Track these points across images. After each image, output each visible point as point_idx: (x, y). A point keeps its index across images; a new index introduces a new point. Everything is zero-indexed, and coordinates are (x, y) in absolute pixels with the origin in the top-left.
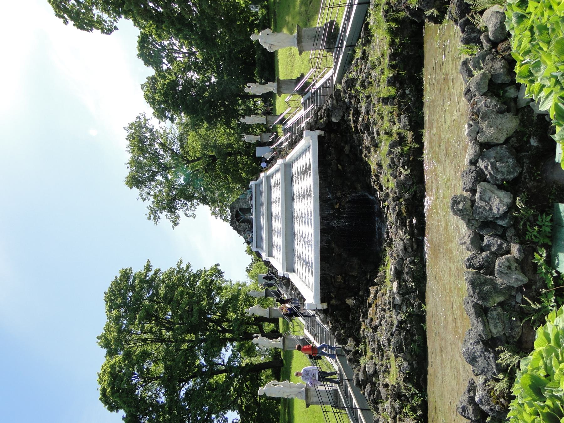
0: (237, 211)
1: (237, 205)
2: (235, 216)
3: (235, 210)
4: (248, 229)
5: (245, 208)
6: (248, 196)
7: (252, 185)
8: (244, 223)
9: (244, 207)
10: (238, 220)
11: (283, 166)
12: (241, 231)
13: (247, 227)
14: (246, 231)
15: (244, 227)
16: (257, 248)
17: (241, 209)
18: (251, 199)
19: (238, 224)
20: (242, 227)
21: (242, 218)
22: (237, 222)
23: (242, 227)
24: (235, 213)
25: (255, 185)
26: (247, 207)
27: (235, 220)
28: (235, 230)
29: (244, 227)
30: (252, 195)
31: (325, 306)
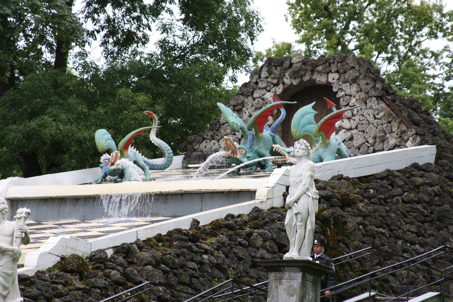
2: (306, 78)
3: (333, 77)
22: (279, 90)
24: (321, 79)
27: (287, 81)
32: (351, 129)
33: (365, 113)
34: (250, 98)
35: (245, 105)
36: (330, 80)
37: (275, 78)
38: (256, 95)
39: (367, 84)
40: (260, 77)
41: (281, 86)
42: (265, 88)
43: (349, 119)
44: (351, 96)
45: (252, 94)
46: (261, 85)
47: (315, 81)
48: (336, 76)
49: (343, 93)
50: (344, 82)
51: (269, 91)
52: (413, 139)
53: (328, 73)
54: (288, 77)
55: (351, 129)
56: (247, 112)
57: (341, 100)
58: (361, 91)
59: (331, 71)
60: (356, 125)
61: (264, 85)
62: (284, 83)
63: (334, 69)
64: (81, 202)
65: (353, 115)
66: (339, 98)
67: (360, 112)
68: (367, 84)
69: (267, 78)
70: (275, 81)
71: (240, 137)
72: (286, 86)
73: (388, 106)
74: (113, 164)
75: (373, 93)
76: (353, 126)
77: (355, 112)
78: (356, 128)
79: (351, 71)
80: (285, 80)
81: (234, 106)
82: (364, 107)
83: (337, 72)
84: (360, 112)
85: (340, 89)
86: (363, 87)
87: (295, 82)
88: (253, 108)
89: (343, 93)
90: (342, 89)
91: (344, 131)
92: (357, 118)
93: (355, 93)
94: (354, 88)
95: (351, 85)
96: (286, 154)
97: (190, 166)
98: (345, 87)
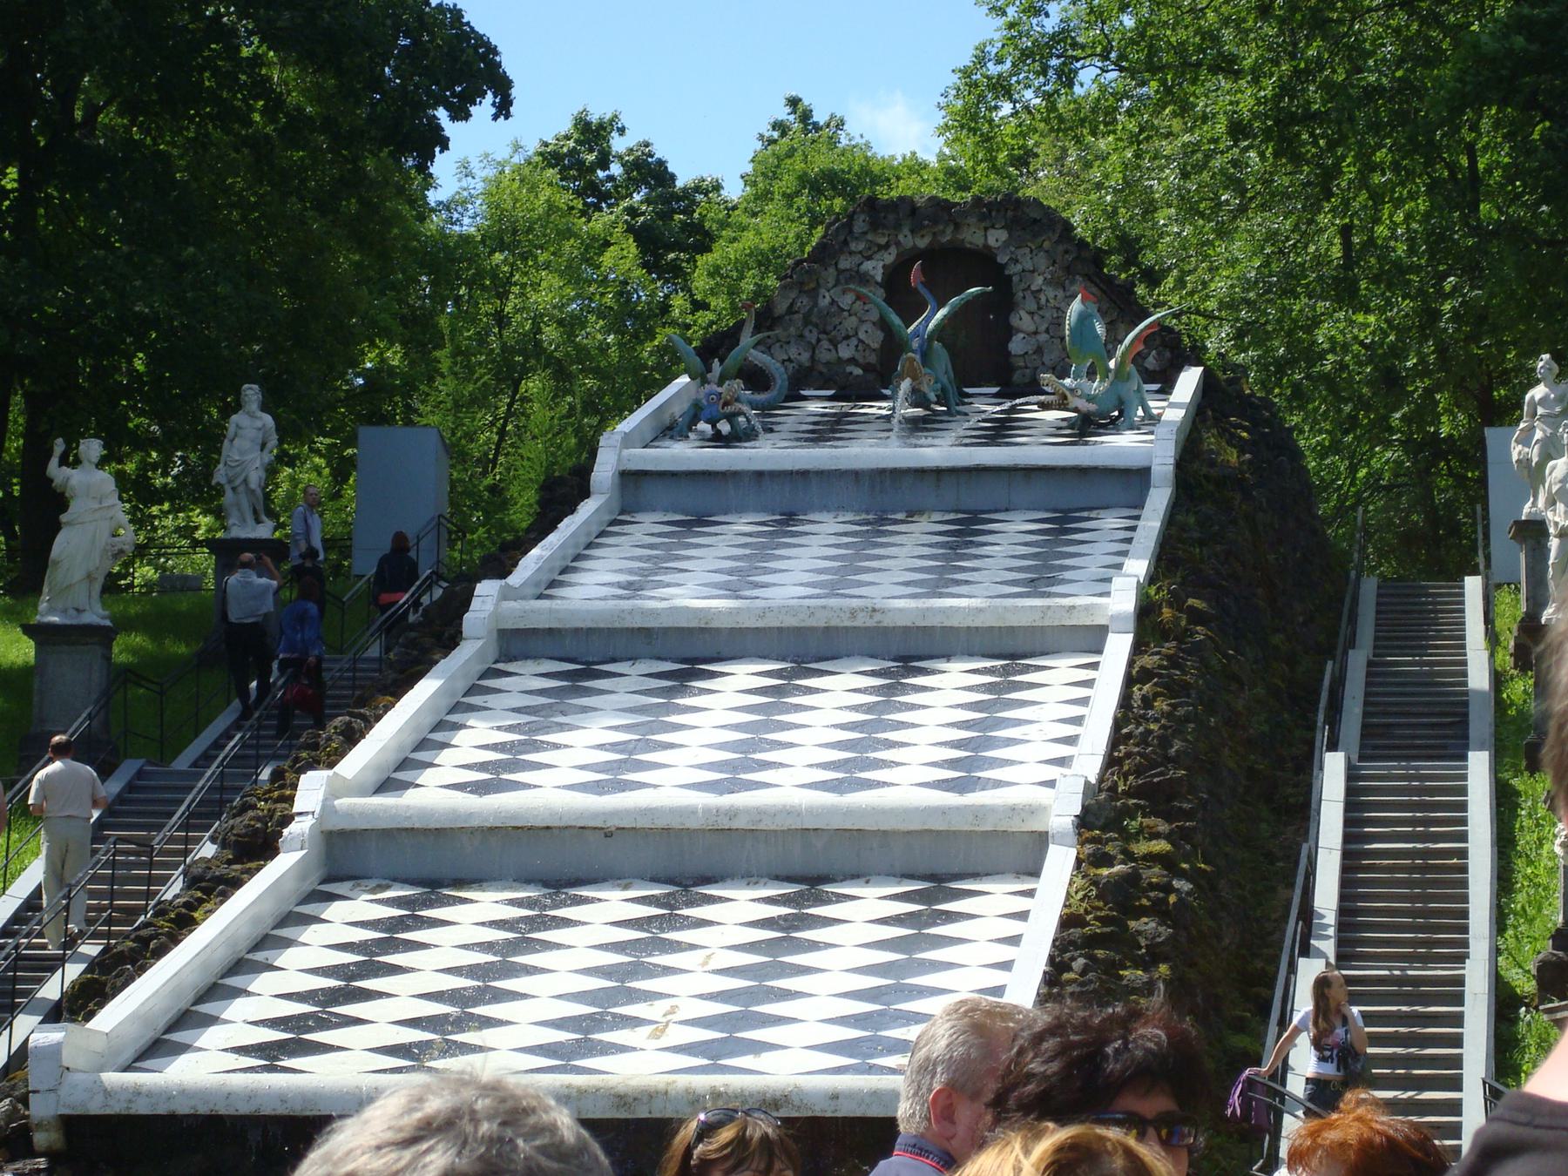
1: (1042, 261)
3: (996, 237)
4: (824, 355)
5: (1010, 332)
12: (813, 294)
13: (845, 352)
14: (812, 337)
17: (1003, 300)
19: (875, 268)
20: (846, 301)
22: (890, 257)
23: (846, 301)
24: (973, 236)
26: (1016, 346)
27: (907, 239)
32: (1036, 333)
34: (832, 270)
35: (821, 281)
36: (992, 242)
37: (883, 234)
39: (1066, 252)
40: (851, 232)
41: (893, 250)
42: (860, 252)
43: (1031, 314)
44: (1033, 272)
45: (836, 264)
46: (853, 246)
49: (1019, 267)
51: (869, 258)
52: (1158, 354)
53: (986, 229)
54: (908, 234)
55: (1036, 333)
56: (827, 294)
57: (1015, 279)
58: (1054, 262)
59: (993, 227)
60: (1046, 325)
61: (861, 246)
62: (898, 244)
65: (1040, 308)
66: (1010, 277)
68: (1066, 252)
69: (865, 233)
70: (883, 241)
71: (814, 341)
72: (901, 249)
73: (1104, 292)
74: (726, 404)
76: (1043, 328)
77: (1043, 301)
78: (1047, 331)
80: (901, 237)
85: (1011, 259)
88: (840, 288)
89: (1019, 267)
90: (1017, 261)
91: (1022, 335)
93: (1043, 268)
95: (1031, 251)
96: (1068, 393)
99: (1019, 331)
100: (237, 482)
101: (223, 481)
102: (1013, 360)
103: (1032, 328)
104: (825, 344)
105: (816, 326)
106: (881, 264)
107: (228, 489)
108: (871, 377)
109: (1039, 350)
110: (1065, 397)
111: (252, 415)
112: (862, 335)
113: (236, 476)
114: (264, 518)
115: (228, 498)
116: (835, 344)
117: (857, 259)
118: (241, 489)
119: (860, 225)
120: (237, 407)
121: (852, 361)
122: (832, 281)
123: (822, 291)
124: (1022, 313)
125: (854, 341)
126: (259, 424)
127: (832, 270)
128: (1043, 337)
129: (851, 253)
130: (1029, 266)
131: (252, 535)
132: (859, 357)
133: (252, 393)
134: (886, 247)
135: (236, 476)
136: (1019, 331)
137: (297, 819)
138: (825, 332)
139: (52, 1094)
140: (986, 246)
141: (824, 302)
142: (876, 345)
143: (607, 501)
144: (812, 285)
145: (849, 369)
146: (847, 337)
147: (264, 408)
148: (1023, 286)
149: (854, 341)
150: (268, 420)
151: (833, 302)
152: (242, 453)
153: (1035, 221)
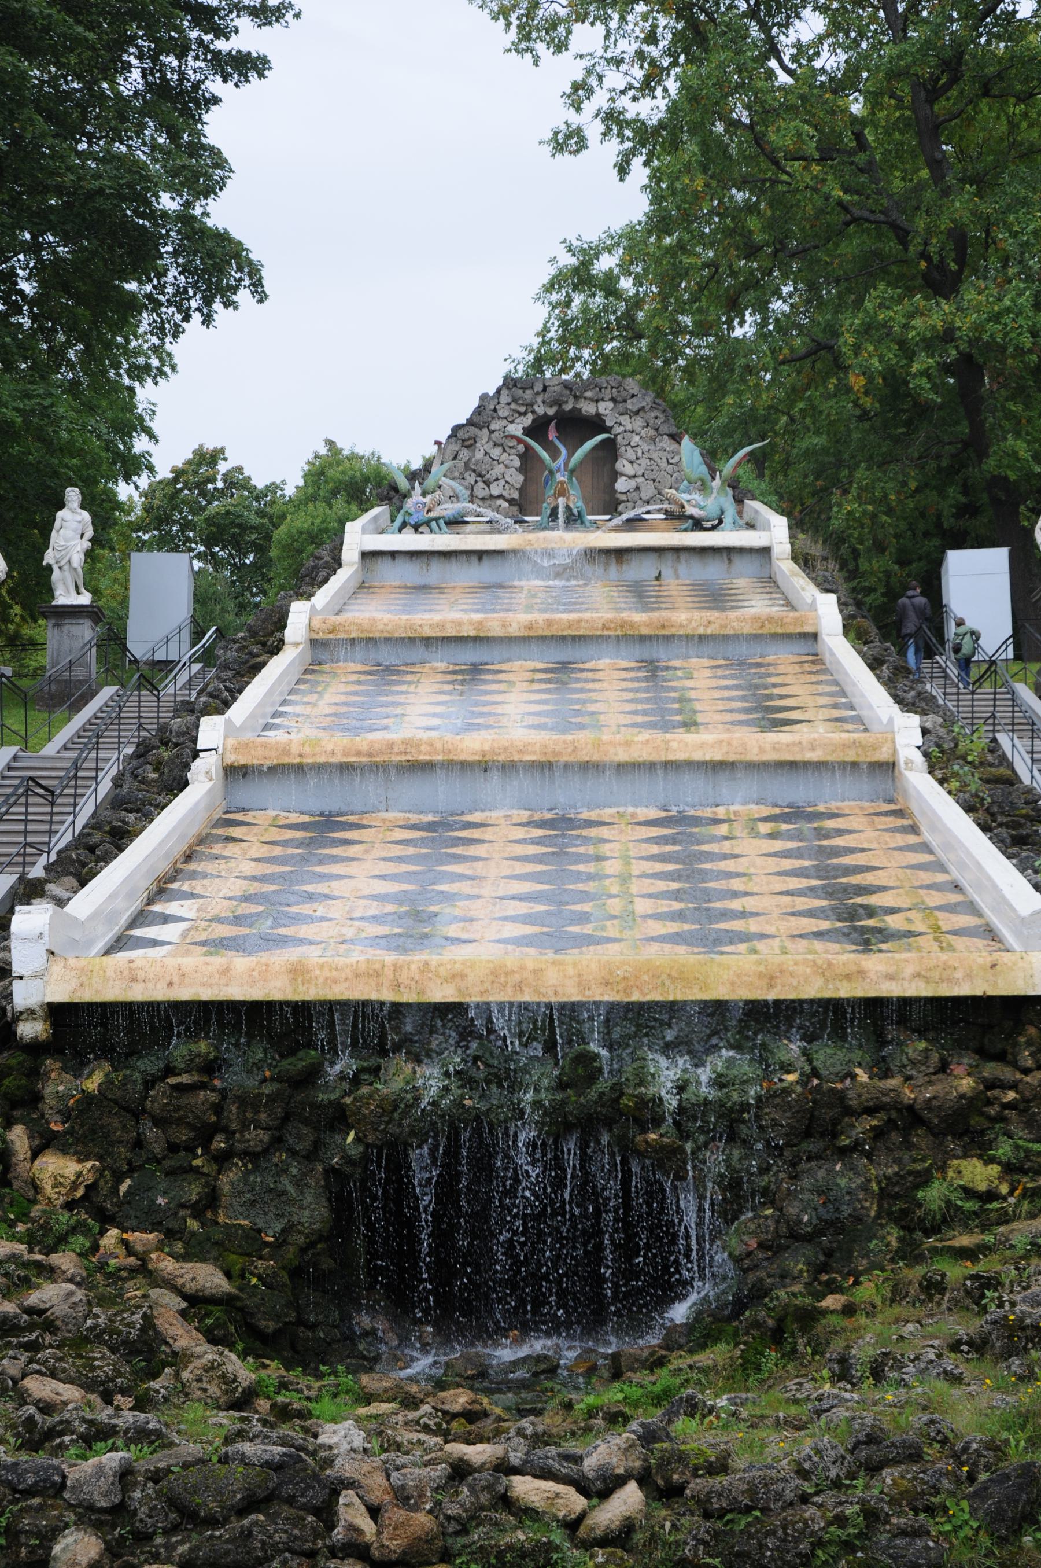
0: (597, 425)
2: (568, 407)
3: (605, 408)
5: (615, 475)
6: (696, 497)
7: (767, 527)
8: (522, 470)
9: (623, 465)
10: (537, 430)
11: (883, 755)
13: (496, 490)
14: (471, 478)
15: (499, 469)
16: (367, 556)
17: (610, 450)
18: (678, 518)
19: (516, 429)
20: (496, 452)
21: (555, 454)
22: (528, 420)
24: (588, 409)
25: (765, 552)
26: (622, 485)
27: (540, 410)
28: (479, 410)
29: (499, 469)
30: (698, 525)
31: (29, 1030)
32: (635, 476)
33: (655, 456)
34: (485, 431)
36: (601, 410)
38: (493, 427)
43: (631, 462)
46: (501, 413)
47: (580, 410)
48: (611, 405)
49: (622, 429)
50: (622, 414)
51: (512, 422)
53: (597, 401)
55: (635, 476)
57: (619, 438)
61: (506, 414)
62: (533, 412)
63: (607, 394)
64: (486, 561)
67: (647, 455)
70: (522, 409)
74: (429, 511)
75: (664, 429)
76: (640, 473)
77: (640, 454)
79: (635, 400)
80: (536, 408)
81: (463, 441)
82: (652, 447)
83: (613, 399)
84: (647, 455)
86: (651, 423)
87: (551, 412)
89: (622, 429)
92: (644, 462)
94: (638, 423)
97: (526, 518)
98: (625, 420)
99: (622, 475)
100: (62, 563)
101: (52, 562)
102: (618, 496)
103: (632, 473)
104: (481, 484)
105: (474, 471)
106: (521, 426)
107: (55, 568)
108: (516, 508)
109: (637, 488)
110: (683, 507)
111: (73, 511)
112: (508, 478)
113: (63, 558)
114: (83, 590)
115: (56, 575)
116: (487, 484)
117: (504, 422)
118: (66, 568)
119: (505, 398)
120: (61, 506)
121: (501, 497)
122: (485, 440)
123: (478, 445)
124: (626, 462)
125: (502, 482)
126: (79, 518)
127: (485, 431)
128: (640, 480)
129: (499, 418)
130: (629, 427)
131: (75, 603)
132: (505, 493)
133: (73, 495)
134: (525, 414)
135: (63, 558)
136: (622, 475)
137: (201, 754)
138: (480, 475)
139: (37, 981)
140: (598, 415)
141: (479, 455)
142: (518, 486)
143: (356, 571)
144: (471, 442)
145: (500, 502)
146: (497, 479)
147: (82, 507)
148: (625, 442)
149: (502, 482)
150: (86, 516)
151: (486, 453)
152: (66, 540)
153: (633, 396)
